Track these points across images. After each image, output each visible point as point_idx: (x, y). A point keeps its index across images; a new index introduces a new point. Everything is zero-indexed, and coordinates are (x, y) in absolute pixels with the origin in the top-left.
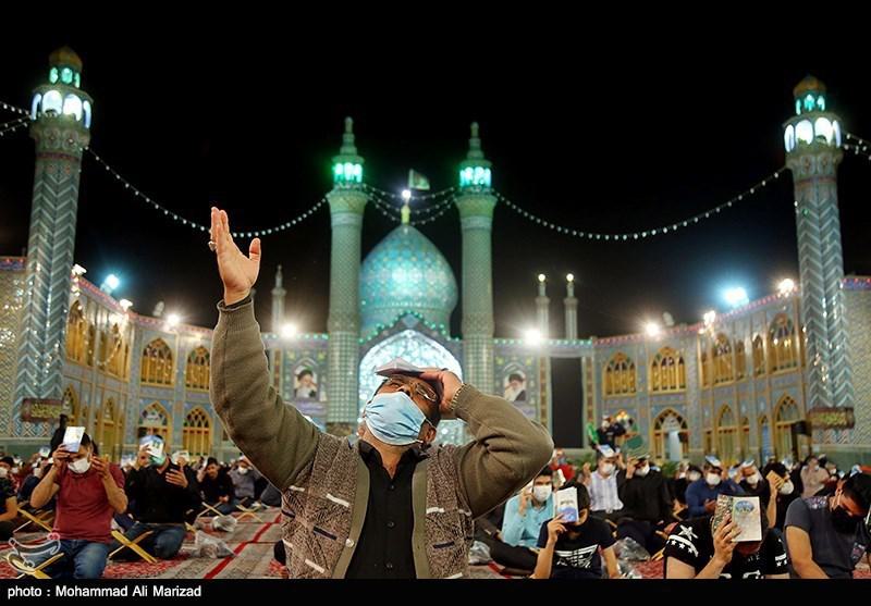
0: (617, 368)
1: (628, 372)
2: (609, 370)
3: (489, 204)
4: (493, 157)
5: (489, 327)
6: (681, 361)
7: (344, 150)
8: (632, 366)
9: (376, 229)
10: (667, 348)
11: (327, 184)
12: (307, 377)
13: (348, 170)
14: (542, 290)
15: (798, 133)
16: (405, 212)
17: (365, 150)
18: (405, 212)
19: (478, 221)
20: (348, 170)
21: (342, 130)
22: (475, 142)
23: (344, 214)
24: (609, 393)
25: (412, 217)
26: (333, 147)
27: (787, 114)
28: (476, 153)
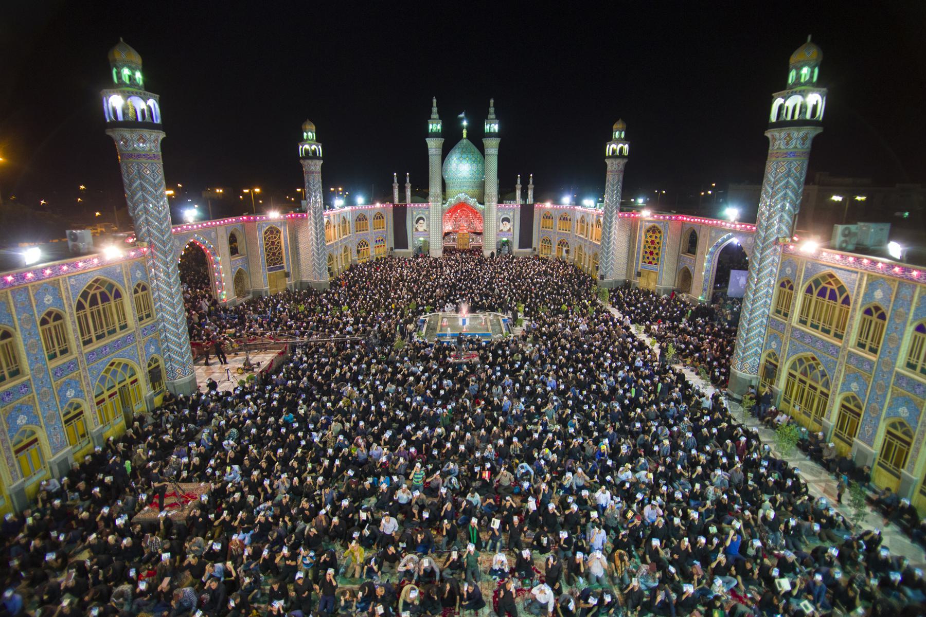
4: (499, 117)
5: (495, 199)
9: (450, 141)
12: (421, 221)
13: (435, 126)
15: (612, 148)
16: (465, 132)
18: (465, 132)
19: (492, 147)
20: (435, 126)
22: (492, 110)
23: (434, 146)
25: (468, 137)
26: (428, 116)
27: (609, 138)
28: (492, 116)
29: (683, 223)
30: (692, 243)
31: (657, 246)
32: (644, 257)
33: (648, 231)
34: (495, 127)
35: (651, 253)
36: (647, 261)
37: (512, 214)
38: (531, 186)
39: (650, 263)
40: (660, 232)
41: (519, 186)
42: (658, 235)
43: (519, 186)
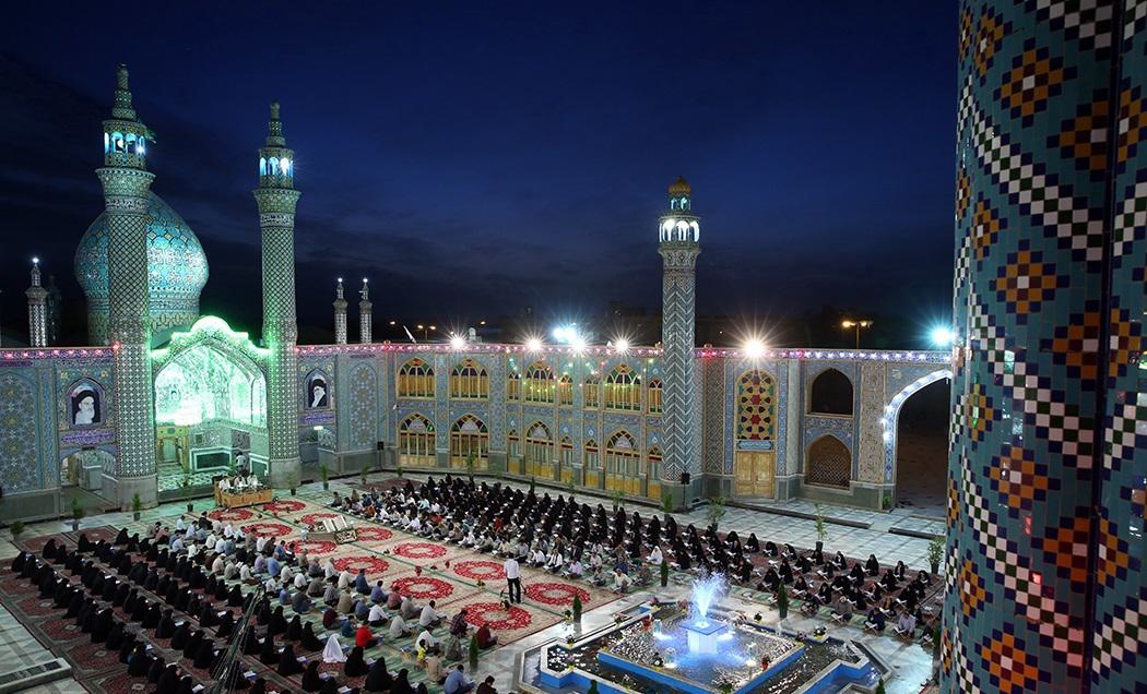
0: (413, 372)
1: (425, 378)
2: (403, 372)
3: (291, 198)
6: (484, 373)
7: (118, 112)
8: (431, 373)
10: (469, 361)
11: (98, 157)
14: (340, 292)
17: (147, 115)
21: (114, 85)
24: (401, 394)
28: (281, 141)
29: (803, 363)
30: (832, 393)
31: (765, 405)
32: (740, 429)
33: (744, 380)
34: (285, 165)
35: (756, 420)
36: (748, 435)
37: (330, 368)
38: (366, 305)
39: (755, 437)
40: (768, 381)
41: (341, 305)
42: (767, 386)
43: (341, 305)
